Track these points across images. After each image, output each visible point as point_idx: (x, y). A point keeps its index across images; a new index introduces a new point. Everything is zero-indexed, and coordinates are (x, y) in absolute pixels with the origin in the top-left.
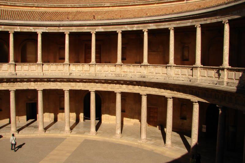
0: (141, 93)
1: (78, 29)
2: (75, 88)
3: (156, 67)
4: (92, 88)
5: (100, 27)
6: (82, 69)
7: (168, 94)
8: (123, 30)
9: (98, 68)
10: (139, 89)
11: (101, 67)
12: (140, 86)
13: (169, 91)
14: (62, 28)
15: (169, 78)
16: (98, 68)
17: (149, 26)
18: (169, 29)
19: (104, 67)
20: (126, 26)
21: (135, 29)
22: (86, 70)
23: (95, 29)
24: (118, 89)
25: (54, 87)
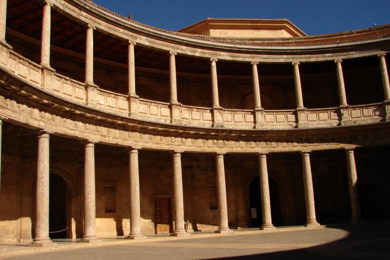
0: (218, 151)
1: (108, 28)
2: (107, 138)
3: (235, 112)
4: (136, 143)
5: (144, 38)
6: (114, 103)
7: (264, 149)
8: (180, 52)
9: (142, 108)
10: (214, 146)
11: (146, 106)
12: (215, 141)
13: (263, 144)
14: (85, 14)
15: (262, 127)
16: (142, 108)
17: (220, 55)
18: (252, 63)
19: (151, 107)
20: (184, 47)
21: (197, 54)
22: (121, 107)
23: (136, 38)
24: (179, 146)
25: (72, 130)
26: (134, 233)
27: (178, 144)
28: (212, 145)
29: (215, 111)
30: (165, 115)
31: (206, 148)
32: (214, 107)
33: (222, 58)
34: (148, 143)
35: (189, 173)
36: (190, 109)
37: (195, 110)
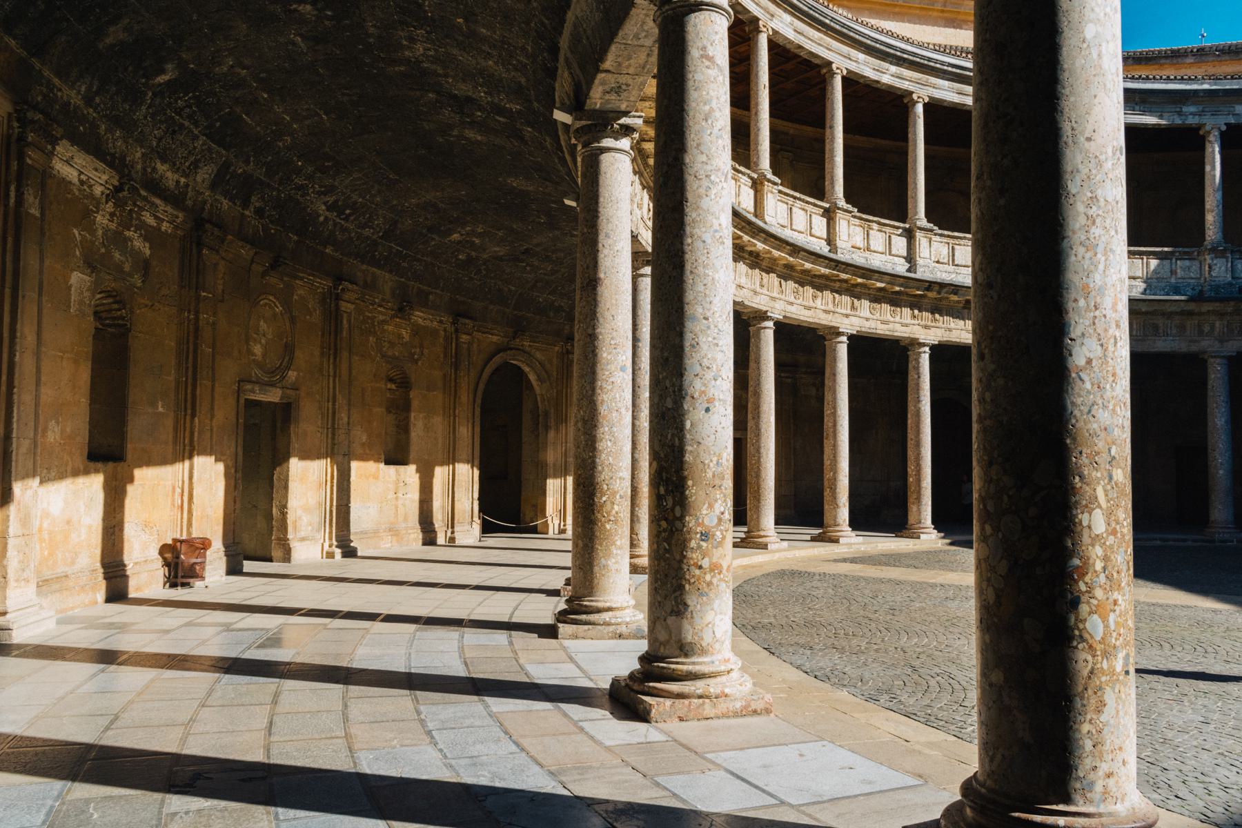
4: (772, 304)
5: (788, 18)
8: (853, 67)
21: (886, 79)
24: (847, 316)
26: (762, 533)
27: (844, 312)
28: (909, 321)
29: (919, 235)
30: (818, 234)
31: (898, 327)
32: (919, 223)
33: (938, 94)
34: (792, 304)
35: (789, 380)
36: (866, 224)
37: (875, 226)
